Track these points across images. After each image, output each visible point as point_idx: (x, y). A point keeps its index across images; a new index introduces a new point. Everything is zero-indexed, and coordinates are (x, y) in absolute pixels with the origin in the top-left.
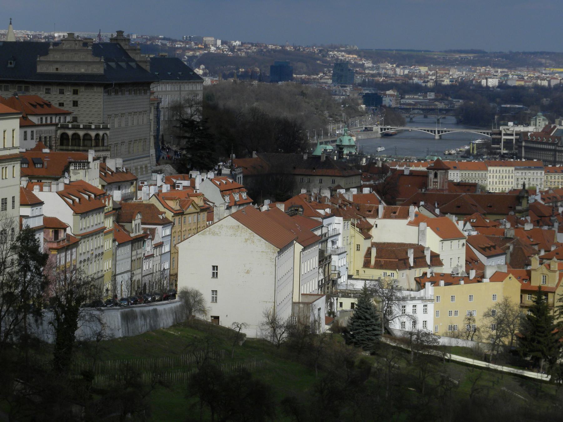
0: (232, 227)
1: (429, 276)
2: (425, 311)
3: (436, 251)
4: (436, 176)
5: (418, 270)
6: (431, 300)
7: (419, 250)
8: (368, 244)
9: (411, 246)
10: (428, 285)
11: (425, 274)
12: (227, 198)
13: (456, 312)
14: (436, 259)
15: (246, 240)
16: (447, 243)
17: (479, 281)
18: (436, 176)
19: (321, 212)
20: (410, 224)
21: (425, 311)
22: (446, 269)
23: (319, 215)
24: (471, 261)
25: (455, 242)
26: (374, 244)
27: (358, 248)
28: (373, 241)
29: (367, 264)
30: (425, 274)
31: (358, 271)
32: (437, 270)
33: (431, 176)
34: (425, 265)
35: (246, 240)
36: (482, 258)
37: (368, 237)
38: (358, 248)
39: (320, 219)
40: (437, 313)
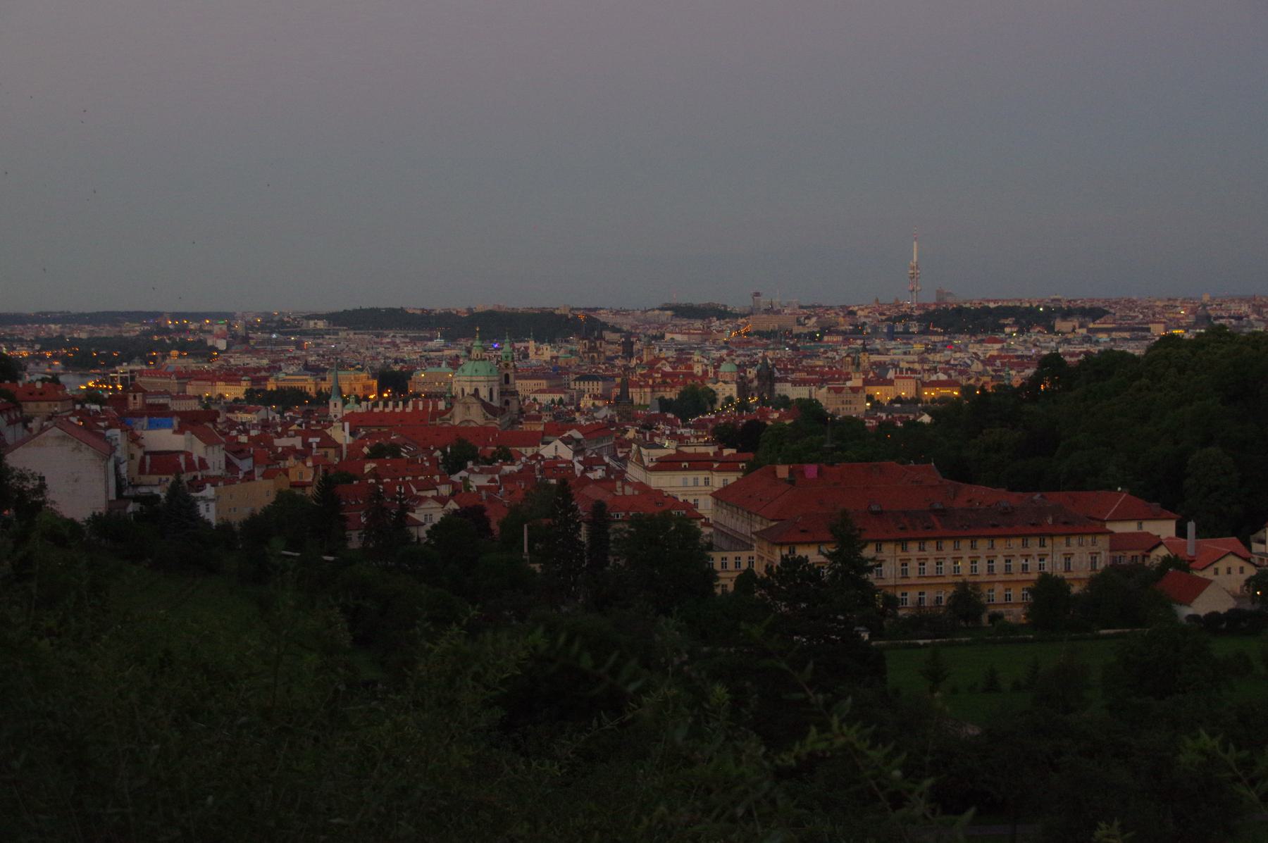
0: (58, 437)
1: (199, 478)
2: (208, 510)
3: (203, 456)
4: (135, 398)
5: (189, 473)
6: (212, 500)
7: (188, 455)
8: (139, 454)
9: (181, 452)
10: (208, 485)
11: (195, 477)
12: (5, 416)
13: (235, 509)
14: (203, 464)
15: (74, 450)
16: (210, 449)
17: (248, 480)
18: (135, 398)
19: (102, 424)
20: (175, 432)
21: (208, 510)
22: (214, 472)
23: (101, 427)
24: (229, 464)
25: (216, 448)
26: (146, 453)
27: (132, 457)
28: (147, 449)
29: (142, 470)
30: (195, 477)
31: (133, 479)
32: (205, 472)
33: (131, 398)
34: (195, 469)
35: (74, 450)
36: (237, 461)
37: (141, 446)
38: (132, 457)
39: (103, 431)
40: (218, 511)
